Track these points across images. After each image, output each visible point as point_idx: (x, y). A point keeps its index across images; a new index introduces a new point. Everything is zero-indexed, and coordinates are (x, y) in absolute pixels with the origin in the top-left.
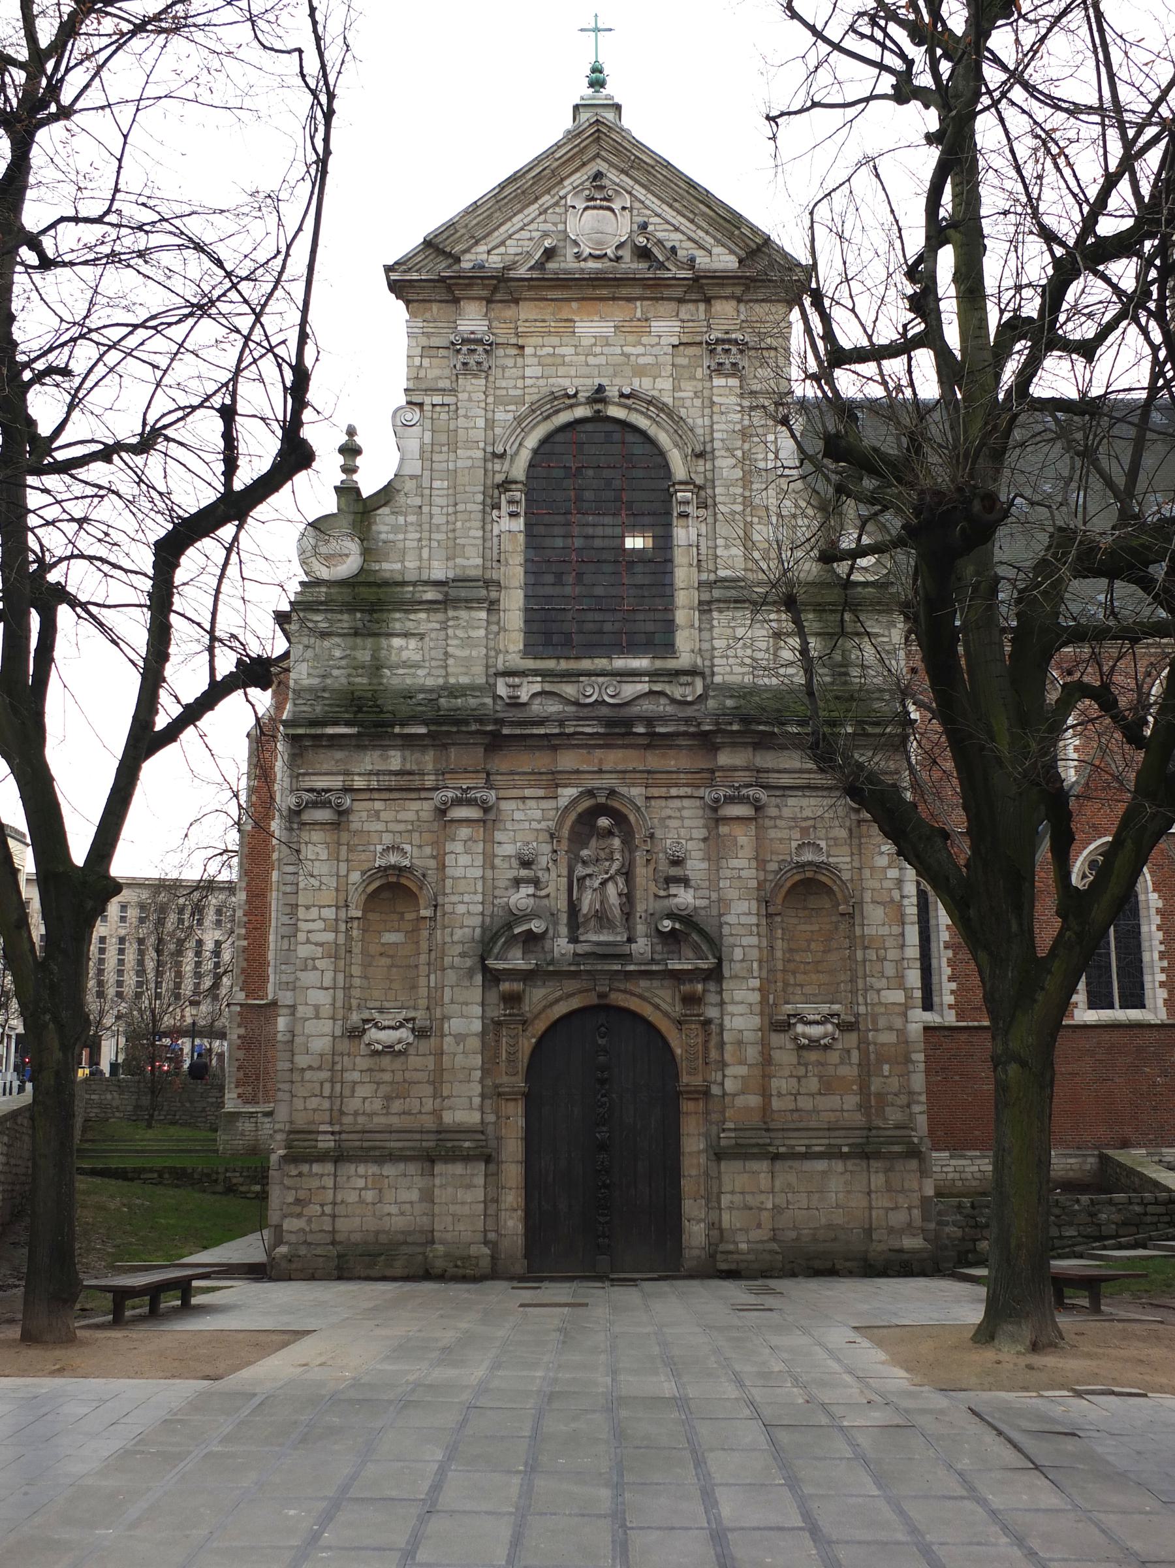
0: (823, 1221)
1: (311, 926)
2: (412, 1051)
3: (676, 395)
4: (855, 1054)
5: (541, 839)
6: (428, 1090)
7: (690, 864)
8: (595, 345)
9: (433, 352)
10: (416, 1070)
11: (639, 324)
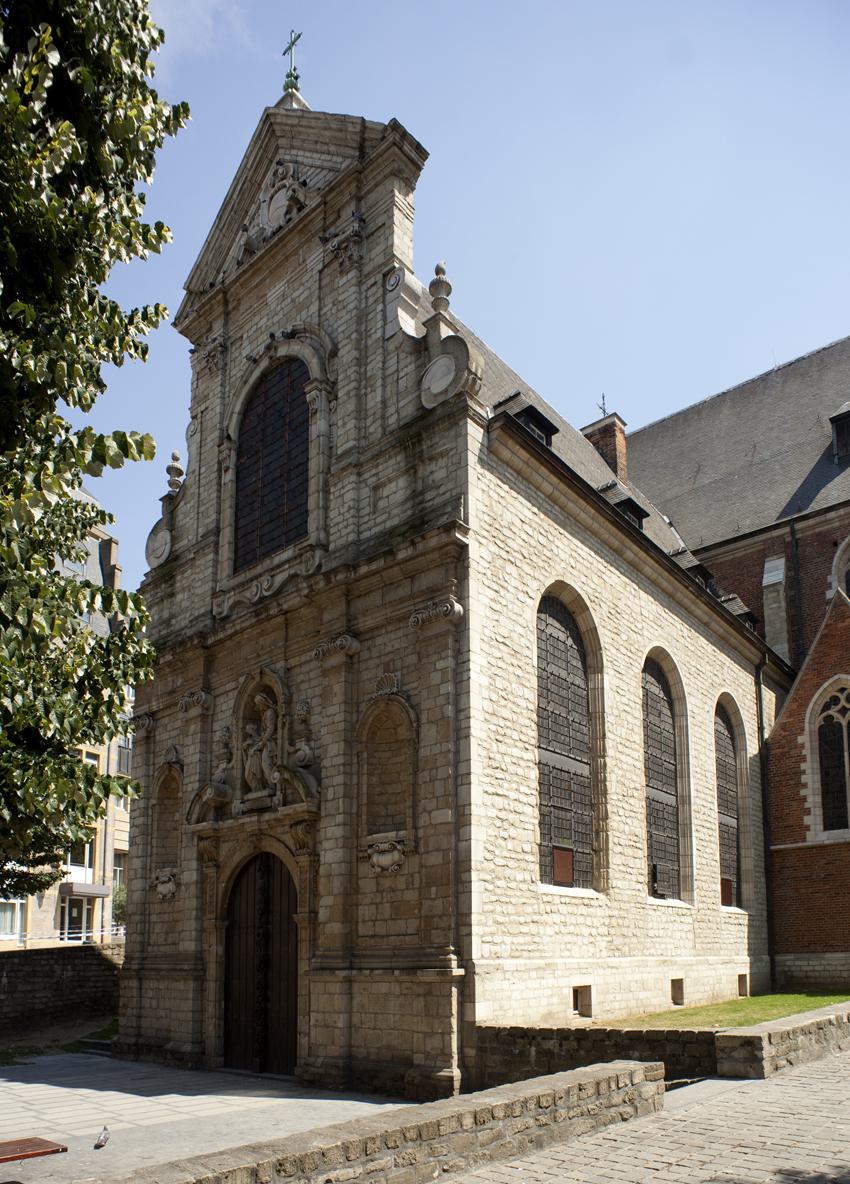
0: (384, 1042)
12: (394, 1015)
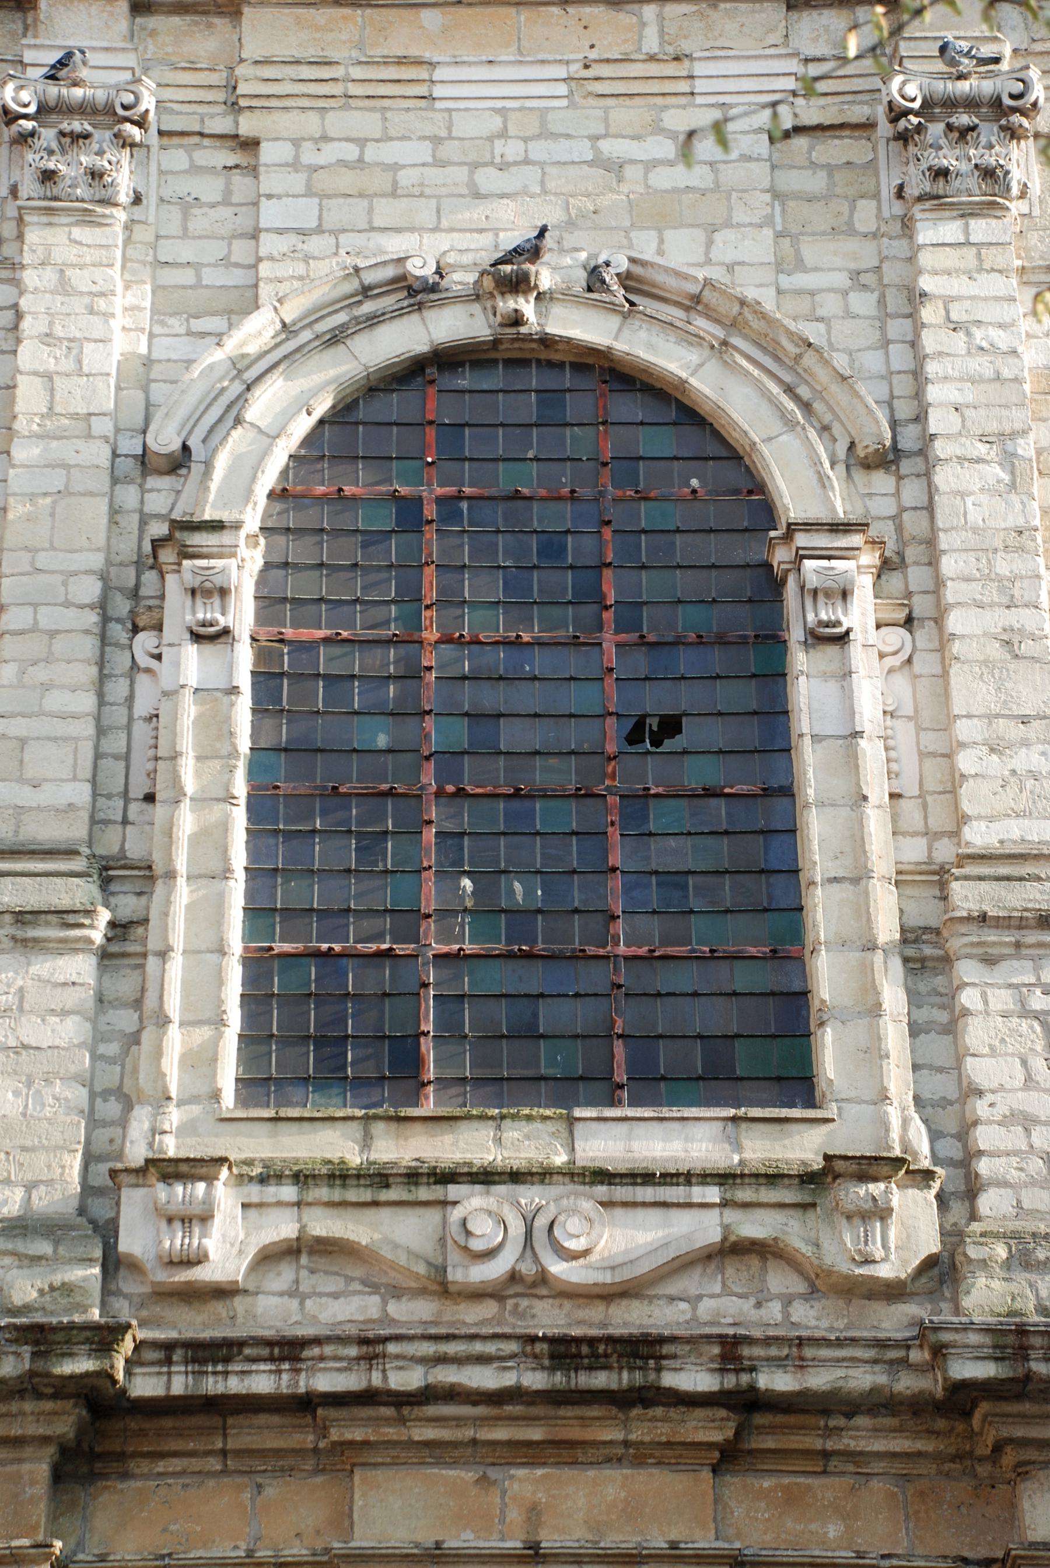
3: (785, 281)
8: (503, 134)
11: (654, 69)
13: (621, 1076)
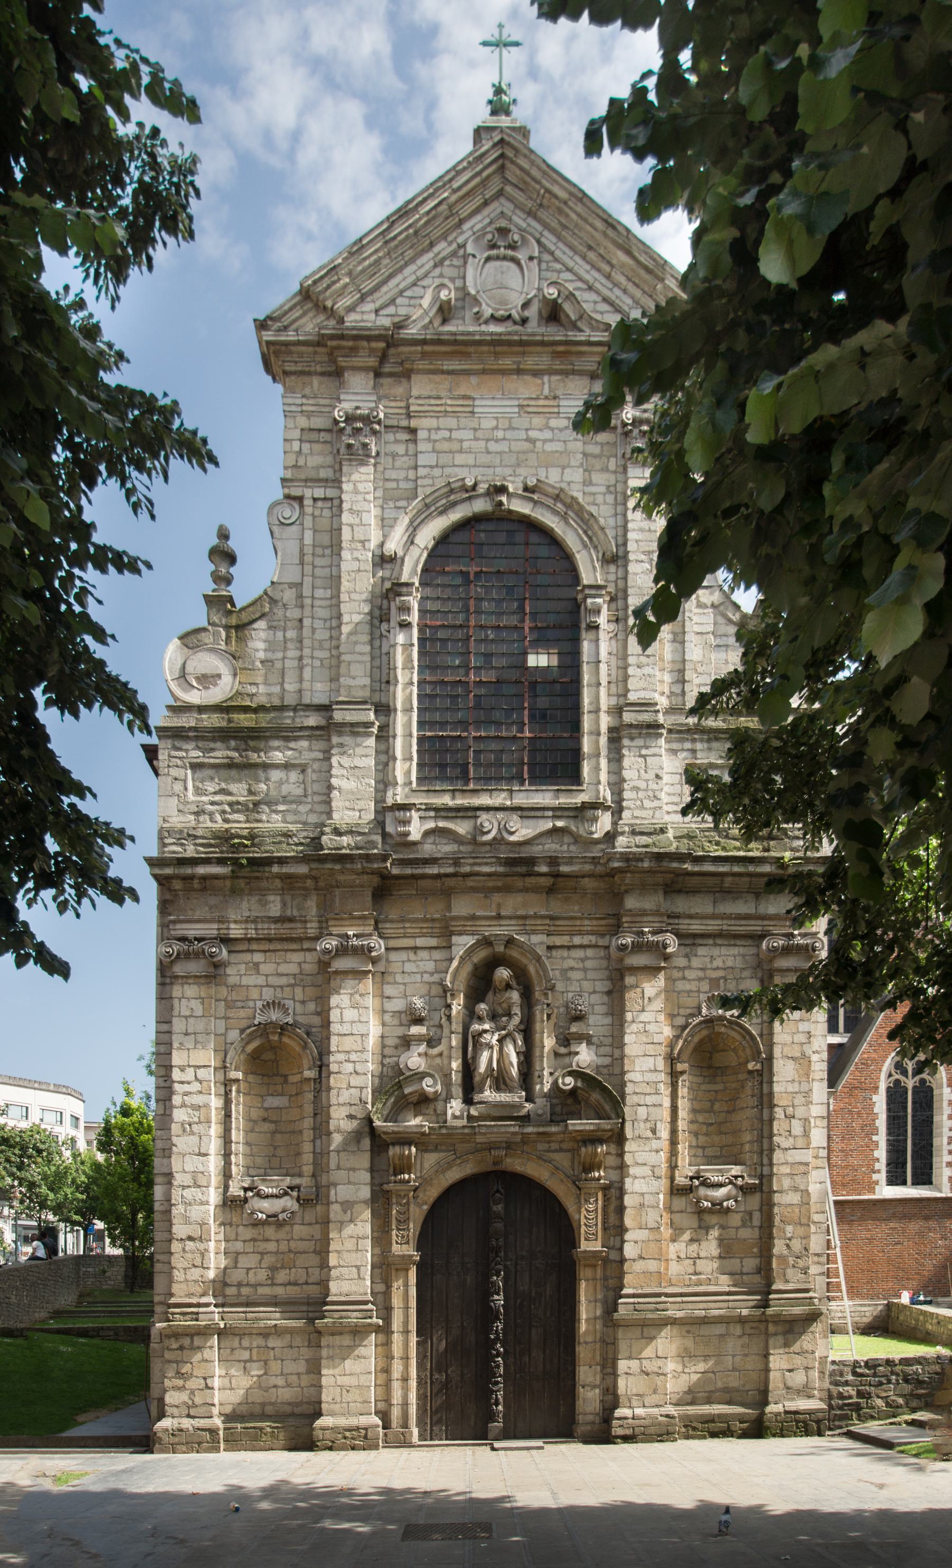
0: (720, 1385)
1: (186, 1088)
2: (298, 1219)
3: (587, 489)
4: (757, 1216)
5: (433, 993)
6: (314, 1260)
7: (592, 1019)
8: (496, 428)
9: (314, 436)
10: (301, 1239)
11: (547, 403)
12: (733, 1356)
13: (526, 776)
